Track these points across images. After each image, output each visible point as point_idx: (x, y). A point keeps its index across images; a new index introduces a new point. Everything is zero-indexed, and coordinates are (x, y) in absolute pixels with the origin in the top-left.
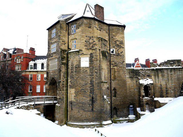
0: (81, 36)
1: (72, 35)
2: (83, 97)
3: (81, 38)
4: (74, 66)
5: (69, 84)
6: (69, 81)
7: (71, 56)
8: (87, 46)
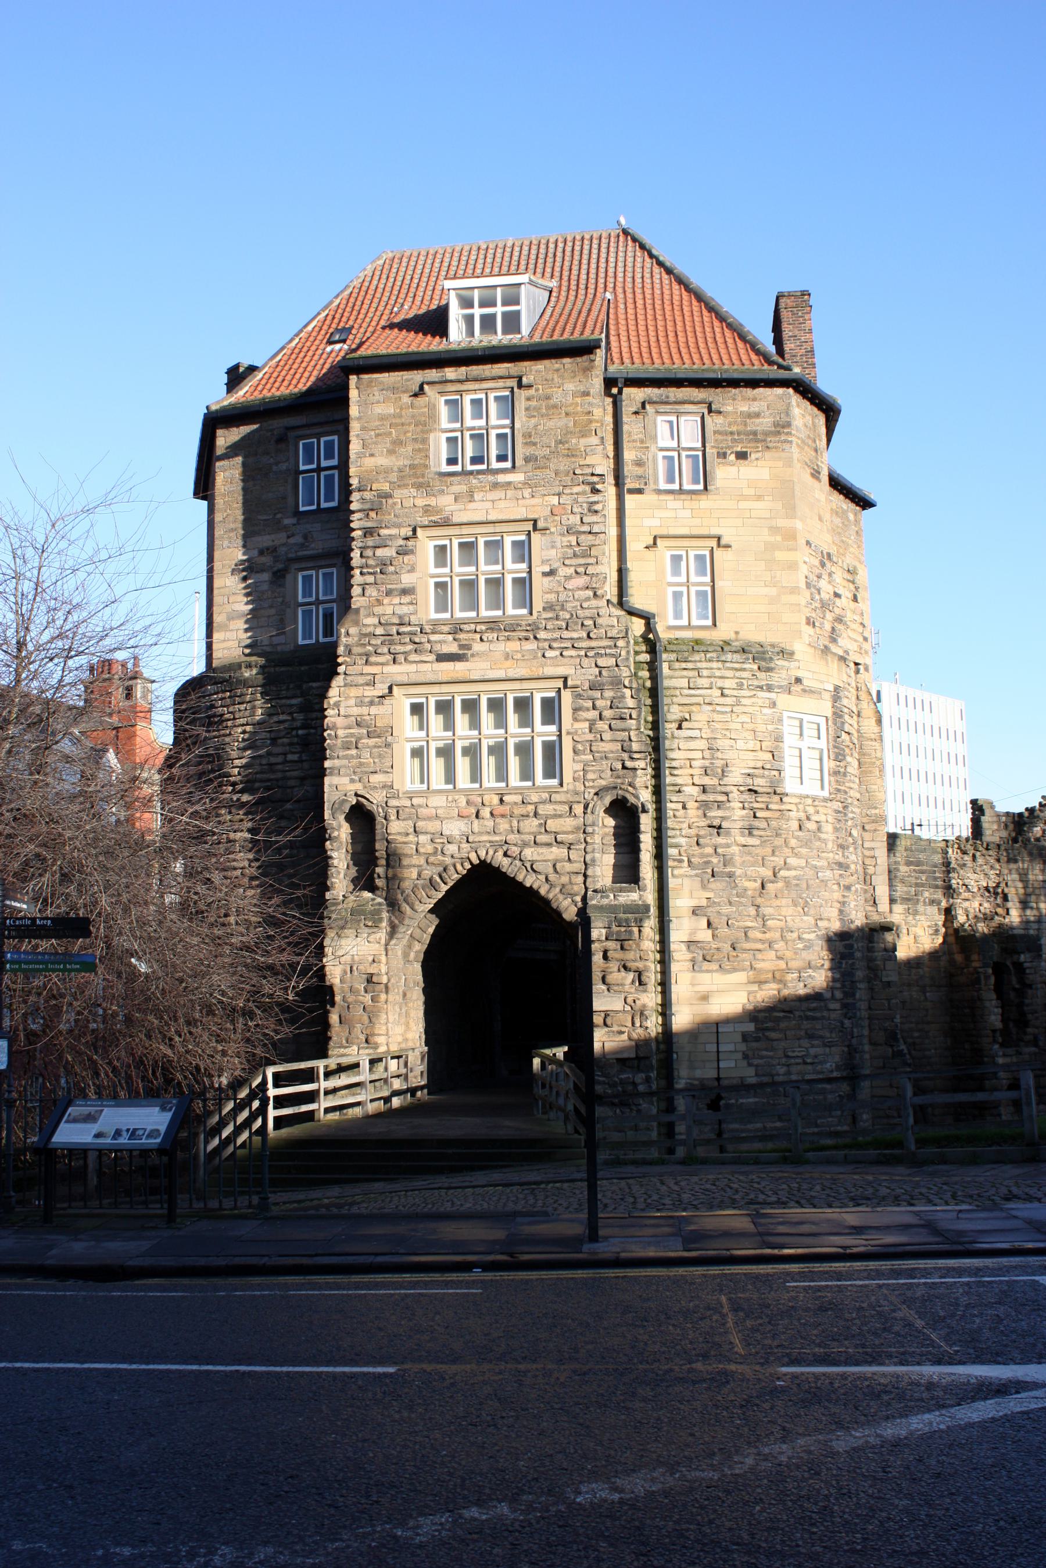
0: (774, 530)
1: (671, 501)
2: (805, 1043)
3: (770, 547)
4: (735, 776)
5: (677, 935)
6: (680, 903)
7: (704, 682)
8: (814, 626)
